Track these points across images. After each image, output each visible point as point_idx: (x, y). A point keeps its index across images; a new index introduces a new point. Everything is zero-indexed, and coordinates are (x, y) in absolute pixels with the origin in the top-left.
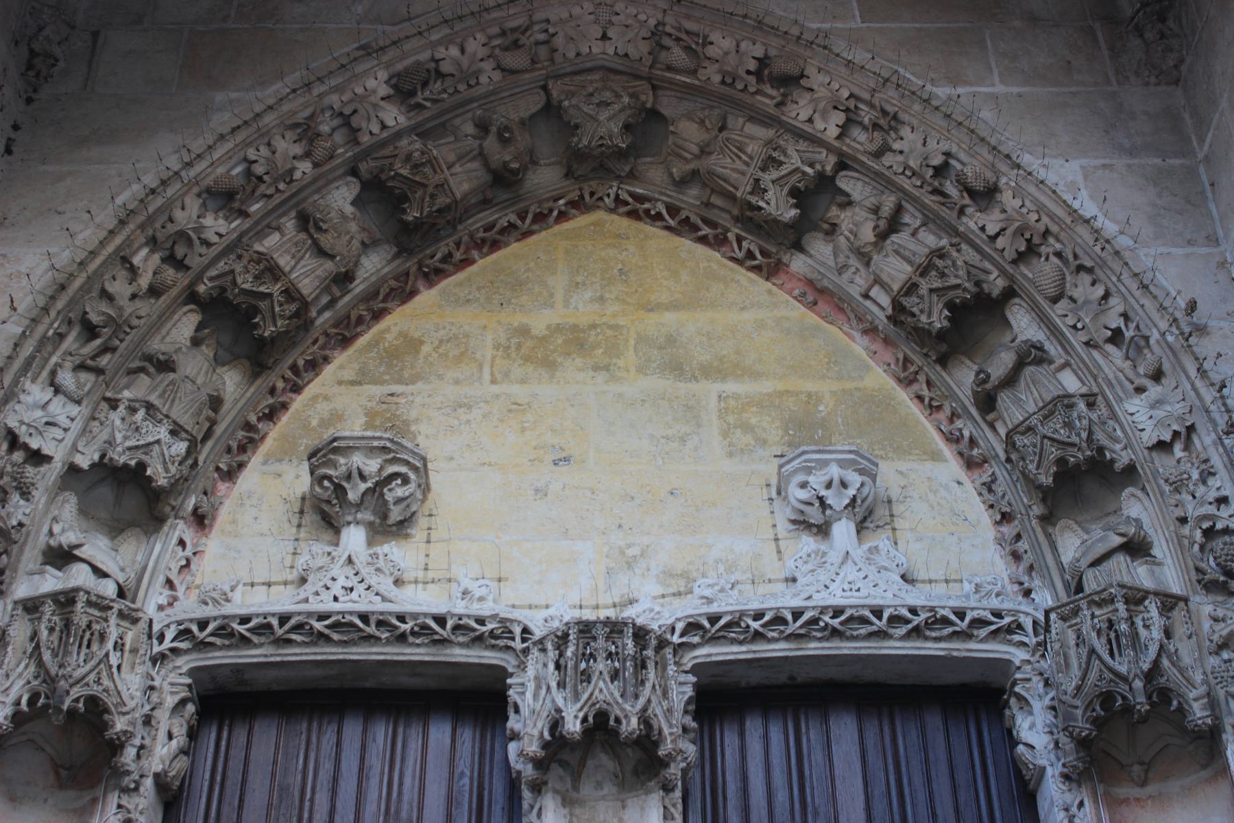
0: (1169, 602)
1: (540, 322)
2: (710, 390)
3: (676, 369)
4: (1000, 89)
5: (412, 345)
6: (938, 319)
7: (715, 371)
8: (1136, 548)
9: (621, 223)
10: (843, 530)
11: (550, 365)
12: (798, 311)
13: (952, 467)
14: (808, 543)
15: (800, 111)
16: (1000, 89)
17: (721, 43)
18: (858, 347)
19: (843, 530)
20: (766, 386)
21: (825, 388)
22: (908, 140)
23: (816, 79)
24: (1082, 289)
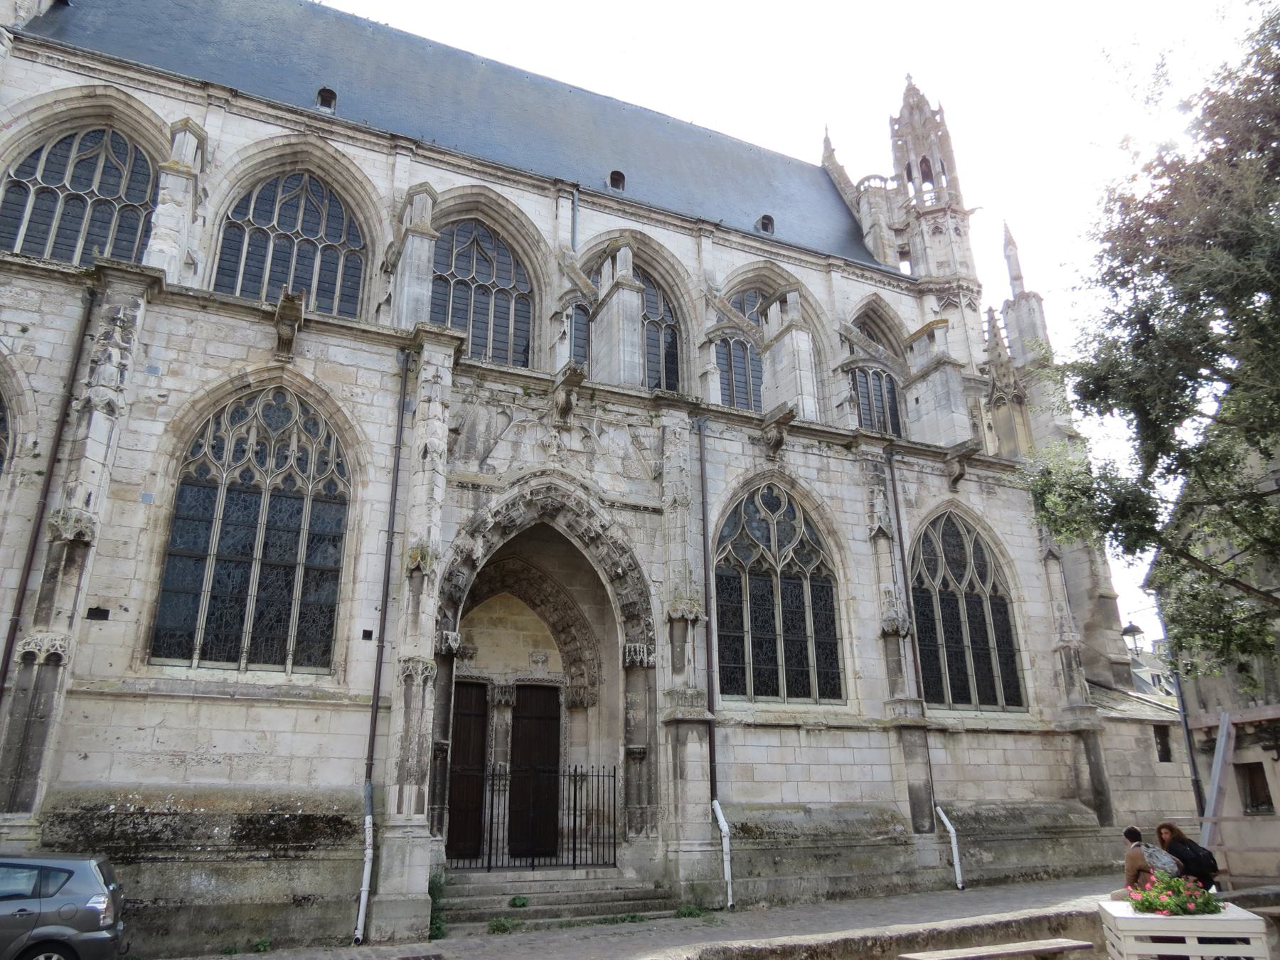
0: (585, 688)
1: (495, 616)
2: (522, 633)
3: (516, 628)
4: (578, 588)
5: (473, 619)
6: (560, 629)
7: (522, 630)
8: (582, 675)
9: (509, 595)
10: (540, 664)
11: (496, 626)
12: (536, 617)
13: (557, 652)
14: (535, 666)
15: (545, 586)
16: (578, 588)
17: (534, 571)
18: (546, 625)
19: (540, 664)
20: (530, 633)
21: (539, 634)
22: (562, 596)
23: (549, 581)
24: (584, 631)
